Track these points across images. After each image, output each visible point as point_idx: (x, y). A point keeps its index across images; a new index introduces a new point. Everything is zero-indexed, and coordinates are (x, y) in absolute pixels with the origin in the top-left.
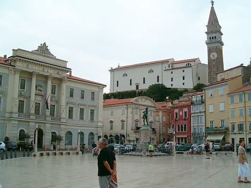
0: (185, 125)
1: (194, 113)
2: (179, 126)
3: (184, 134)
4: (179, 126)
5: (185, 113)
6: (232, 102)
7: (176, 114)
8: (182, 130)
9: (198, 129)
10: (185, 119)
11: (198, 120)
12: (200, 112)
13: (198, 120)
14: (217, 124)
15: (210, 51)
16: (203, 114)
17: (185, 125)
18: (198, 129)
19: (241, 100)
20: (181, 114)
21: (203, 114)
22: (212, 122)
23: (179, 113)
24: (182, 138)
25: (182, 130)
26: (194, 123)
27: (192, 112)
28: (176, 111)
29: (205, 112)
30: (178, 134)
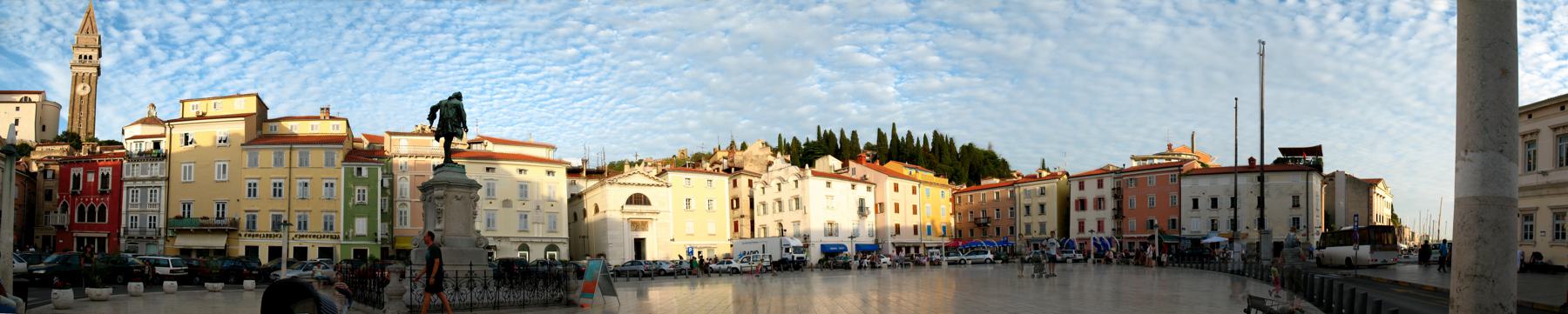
0: (102, 209)
1: (135, 180)
2: (81, 209)
3: (100, 228)
4: (81, 209)
5: (105, 177)
6: (254, 163)
7: (77, 178)
8: (92, 218)
9: (143, 220)
10: (103, 193)
11: (144, 197)
12: (154, 179)
13: (144, 197)
14: (204, 209)
15: (76, 80)
16: (163, 184)
17: (102, 209)
18: (143, 220)
19: (278, 162)
20: (91, 177)
21: (163, 184)
22: (187, 206)
23: (85, 177)
24: (91, 240)
25: (92, 218)
26: (130, 205)
27: (125, 176)
28: (79, 171)
29: (168, 179)
30: (81, 228)
